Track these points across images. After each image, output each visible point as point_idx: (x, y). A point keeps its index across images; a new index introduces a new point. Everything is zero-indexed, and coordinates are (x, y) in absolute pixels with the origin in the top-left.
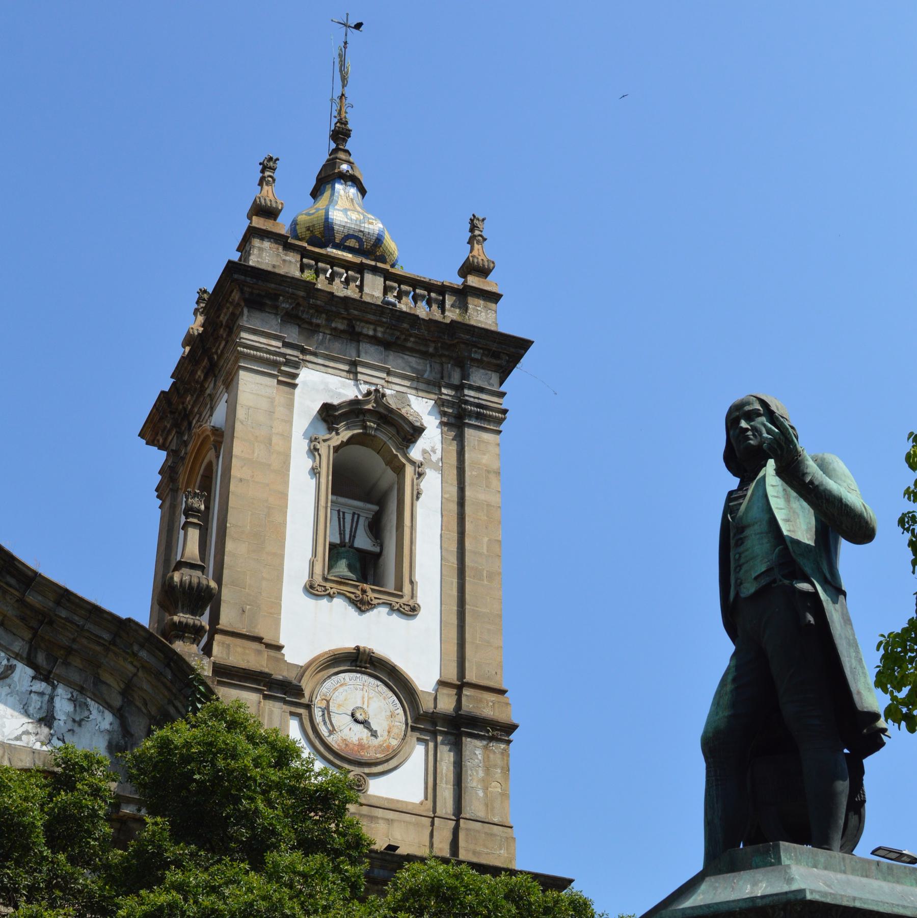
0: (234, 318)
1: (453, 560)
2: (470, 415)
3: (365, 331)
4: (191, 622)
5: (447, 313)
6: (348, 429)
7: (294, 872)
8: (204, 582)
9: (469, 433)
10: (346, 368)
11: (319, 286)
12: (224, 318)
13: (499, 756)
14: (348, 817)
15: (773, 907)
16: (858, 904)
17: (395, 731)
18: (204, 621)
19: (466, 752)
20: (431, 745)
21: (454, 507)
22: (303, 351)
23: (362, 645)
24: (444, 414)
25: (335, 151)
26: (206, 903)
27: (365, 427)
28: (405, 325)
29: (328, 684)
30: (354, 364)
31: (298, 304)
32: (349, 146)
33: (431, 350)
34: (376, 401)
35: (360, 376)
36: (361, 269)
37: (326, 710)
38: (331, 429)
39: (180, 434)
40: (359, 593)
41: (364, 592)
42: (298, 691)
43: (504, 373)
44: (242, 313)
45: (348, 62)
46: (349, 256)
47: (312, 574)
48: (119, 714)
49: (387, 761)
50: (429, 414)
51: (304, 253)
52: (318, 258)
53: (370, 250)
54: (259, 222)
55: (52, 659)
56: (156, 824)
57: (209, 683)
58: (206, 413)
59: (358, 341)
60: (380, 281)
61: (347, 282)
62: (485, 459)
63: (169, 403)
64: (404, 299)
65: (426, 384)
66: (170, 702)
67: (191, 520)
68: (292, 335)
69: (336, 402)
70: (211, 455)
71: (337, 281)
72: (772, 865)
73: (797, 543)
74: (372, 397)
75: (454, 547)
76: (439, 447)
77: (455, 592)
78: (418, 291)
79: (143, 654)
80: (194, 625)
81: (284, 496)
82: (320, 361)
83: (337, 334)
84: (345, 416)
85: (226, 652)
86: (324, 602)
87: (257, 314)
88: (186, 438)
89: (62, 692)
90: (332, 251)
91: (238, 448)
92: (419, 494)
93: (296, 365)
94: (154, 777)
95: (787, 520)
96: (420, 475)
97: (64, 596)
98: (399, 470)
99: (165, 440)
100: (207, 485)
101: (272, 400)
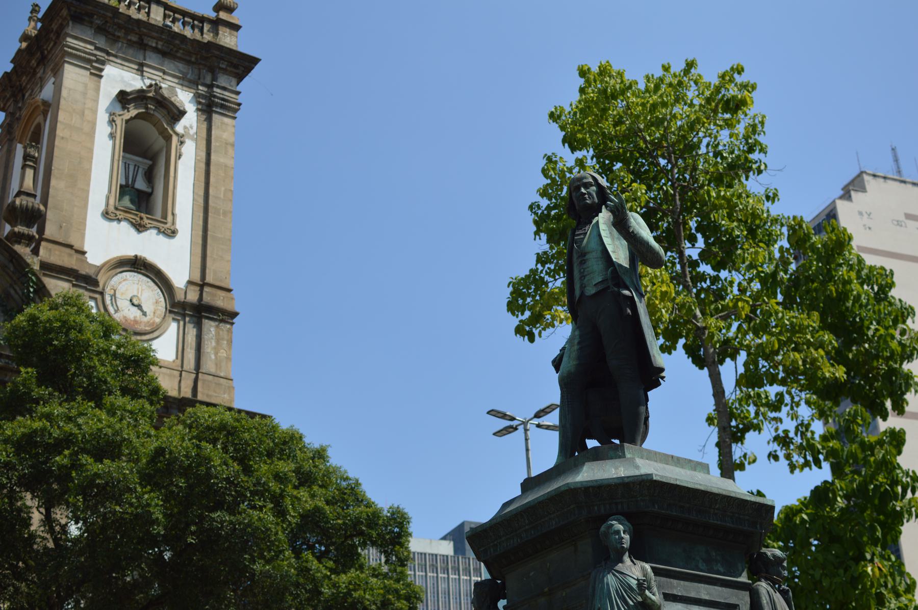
0: (62, 27)
1: (201, 201)
2: (217, 105)
3: (150, 43)
4: (26, 232)
5: (205, 36)
6: (136, 108)
7: (125, 410)
8: (37, 206)
9: (215, 117)
10: (136, 67)
11: (121, 10)
12: (55, 26)
13: (225, 332)
14: (150, 374)
15: (633, 483)
16: (678, 483)
17: (158, 312)
18: (33, 231)
20: (182, 323)
21: (203, 166)
22: (108, 54)
23: (139, 254)
24: (199, 103)
26: (66, 429)
27: (147, 108)
28: (177, 42)
29: (115, 279)
31: (106, 22)
33: (193, 59)
34: (155, 91)
35: (145, 74)
37: (114, 296)
38: (124, 108)
39: (16, 102)
40: (138, 219)
41: (141, 218)
42: (95, 283)
43: (240, 78)
44: (68, 25)
47: (107, 204)
49: (152, 332)
50: (190, 102)
56: (27, 373)
57: (38, 273)
58: (37, 89)
59: (145, 50)
60: (161, 10)
61: (139, 9)
62: (225, 135)
63: (10, 81)
64: (176, 23)
65: (189, 82)
66: (11, 286)
67: (28, 163)
68: (101, 42)
69: (128, 90)
70: (40, 119)
71: (132, 8)
72: (620, 457)
73: (620, 266)
74: (153, 88)
75: (202, 193)
76: (195, 125)
77: (201, 223)
78: (186, 19)
80: (28, 235)
81: (91, 151)
82: (119, 61)
83: (131, 44)
84: (134, 100)
85: (48, 253)
86: (115, 223)
88: (20, 105)
91: (62, 116)
92: (180, 156)
94: (24, 341)
95: (614, 252)
96: (182, 143)
98: (168, 139)
99: (5, 105)
100: (36, 138)
101: (86, 85)
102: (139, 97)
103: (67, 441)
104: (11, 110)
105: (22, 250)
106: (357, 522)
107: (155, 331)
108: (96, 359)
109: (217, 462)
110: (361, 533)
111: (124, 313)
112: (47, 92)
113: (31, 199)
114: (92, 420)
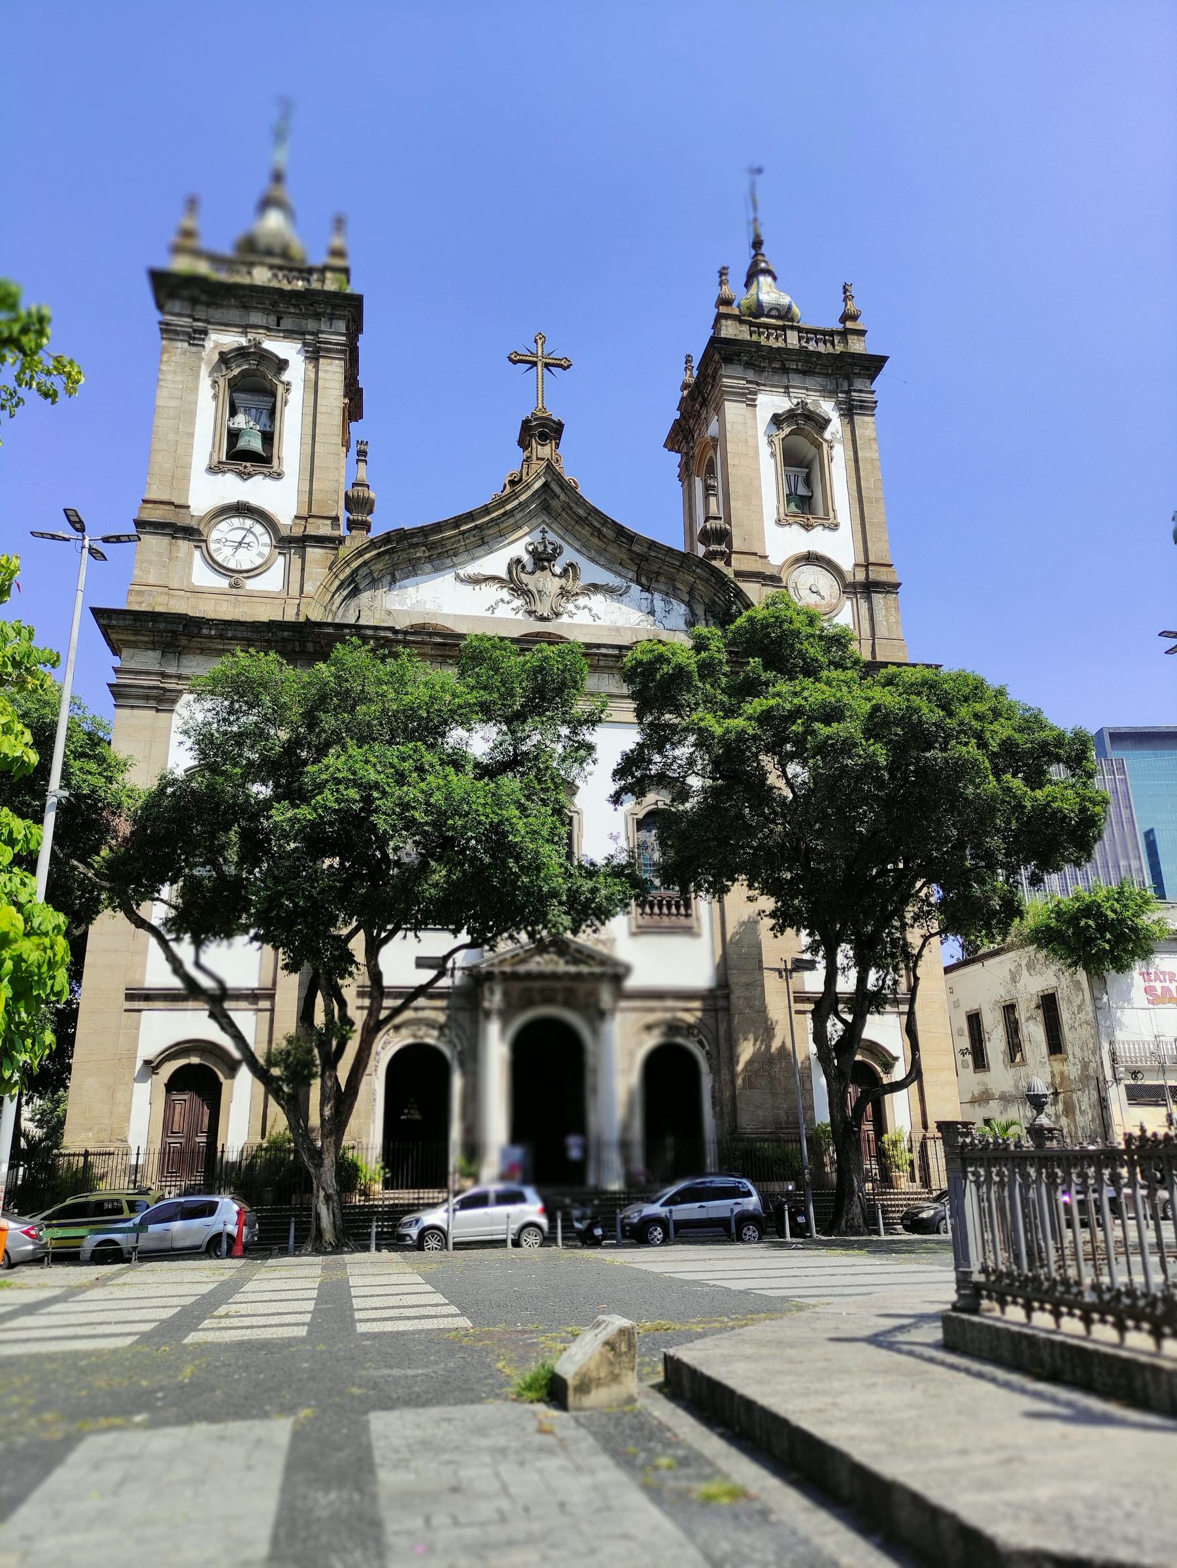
0: (716, 370)
2: (856, 407)
9: (856, 417)
12: (710, 371)
18: (723, 547)
19: (874, 602)
22: (758, 384)
24: (841, 409)
25: (756, 255)
30: (787, 387)
32: (764, 250)
36: (784, 328)
38: (778, 429)
39: (688, 443)
42: (779, 580)
43: (872, 378)
45: (758, 196)
46: (773, 321)
48: (689, 604)
51: (751, 324)
52: (759, 326)
53: (785, 314)
54: (723, 309)
55: (649, 579)
62: (867, 433)
63: (680, 426)
65: (828, 393)
68: (751, 375)
69: (780, 412)
70: (711, 453)
76: (840, 429)
79: (698, 570)
83: (775, 371)
85: (739, 563)
86: (787, 528)
87: (730, 366)
89: (657, 596)
90: (764, 320)
91: (730, 447)
93: (755, 393)
97: (653, 545)
98: (819, 447)
100: (711, 470)
102: (791, 416)
103: (798, 712)
104: (685, 450)
105: (718, 564)
106: (1044, 745)
107: (833, 610)
108: (806, 643)
109: (925, 710)
110: (1049, 754)
111: (807, 600)
112: (713, 429)
113: (718, 522)
114: (815, 693)
